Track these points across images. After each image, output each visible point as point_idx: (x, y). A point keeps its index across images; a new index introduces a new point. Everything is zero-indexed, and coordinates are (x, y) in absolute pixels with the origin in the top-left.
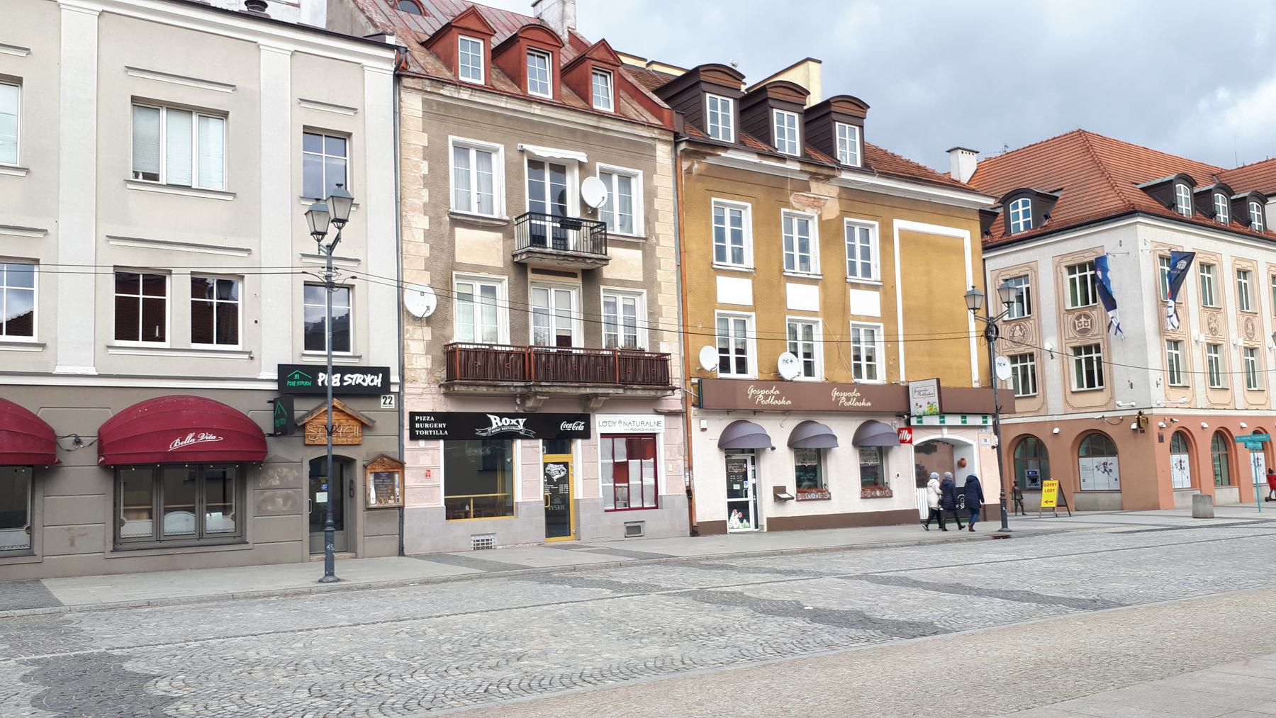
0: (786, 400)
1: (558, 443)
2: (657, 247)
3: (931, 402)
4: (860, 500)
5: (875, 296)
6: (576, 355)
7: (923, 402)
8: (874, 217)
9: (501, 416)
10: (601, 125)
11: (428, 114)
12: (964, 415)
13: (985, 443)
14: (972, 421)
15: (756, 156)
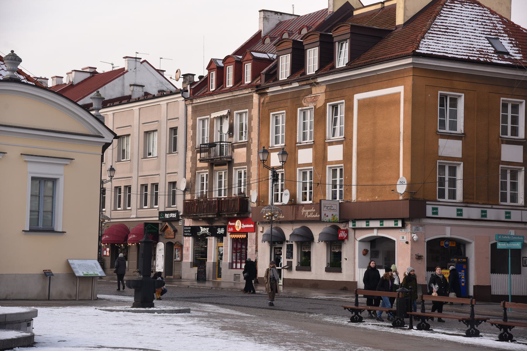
0: (282, 216)
1: (220, 238)
2: (252, 144)
3: (334, 214)
4: (325, 272)
5: (340, 148)
6: (214, 201)
7: (329, 213)
8: (342, 98)
9: (203, 227)
10: (234, 95)
11: (194, 112)
12: (382, 220)
13: (403, 240)
14: (387, 224)
15: (280, 87)
